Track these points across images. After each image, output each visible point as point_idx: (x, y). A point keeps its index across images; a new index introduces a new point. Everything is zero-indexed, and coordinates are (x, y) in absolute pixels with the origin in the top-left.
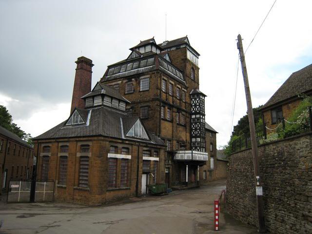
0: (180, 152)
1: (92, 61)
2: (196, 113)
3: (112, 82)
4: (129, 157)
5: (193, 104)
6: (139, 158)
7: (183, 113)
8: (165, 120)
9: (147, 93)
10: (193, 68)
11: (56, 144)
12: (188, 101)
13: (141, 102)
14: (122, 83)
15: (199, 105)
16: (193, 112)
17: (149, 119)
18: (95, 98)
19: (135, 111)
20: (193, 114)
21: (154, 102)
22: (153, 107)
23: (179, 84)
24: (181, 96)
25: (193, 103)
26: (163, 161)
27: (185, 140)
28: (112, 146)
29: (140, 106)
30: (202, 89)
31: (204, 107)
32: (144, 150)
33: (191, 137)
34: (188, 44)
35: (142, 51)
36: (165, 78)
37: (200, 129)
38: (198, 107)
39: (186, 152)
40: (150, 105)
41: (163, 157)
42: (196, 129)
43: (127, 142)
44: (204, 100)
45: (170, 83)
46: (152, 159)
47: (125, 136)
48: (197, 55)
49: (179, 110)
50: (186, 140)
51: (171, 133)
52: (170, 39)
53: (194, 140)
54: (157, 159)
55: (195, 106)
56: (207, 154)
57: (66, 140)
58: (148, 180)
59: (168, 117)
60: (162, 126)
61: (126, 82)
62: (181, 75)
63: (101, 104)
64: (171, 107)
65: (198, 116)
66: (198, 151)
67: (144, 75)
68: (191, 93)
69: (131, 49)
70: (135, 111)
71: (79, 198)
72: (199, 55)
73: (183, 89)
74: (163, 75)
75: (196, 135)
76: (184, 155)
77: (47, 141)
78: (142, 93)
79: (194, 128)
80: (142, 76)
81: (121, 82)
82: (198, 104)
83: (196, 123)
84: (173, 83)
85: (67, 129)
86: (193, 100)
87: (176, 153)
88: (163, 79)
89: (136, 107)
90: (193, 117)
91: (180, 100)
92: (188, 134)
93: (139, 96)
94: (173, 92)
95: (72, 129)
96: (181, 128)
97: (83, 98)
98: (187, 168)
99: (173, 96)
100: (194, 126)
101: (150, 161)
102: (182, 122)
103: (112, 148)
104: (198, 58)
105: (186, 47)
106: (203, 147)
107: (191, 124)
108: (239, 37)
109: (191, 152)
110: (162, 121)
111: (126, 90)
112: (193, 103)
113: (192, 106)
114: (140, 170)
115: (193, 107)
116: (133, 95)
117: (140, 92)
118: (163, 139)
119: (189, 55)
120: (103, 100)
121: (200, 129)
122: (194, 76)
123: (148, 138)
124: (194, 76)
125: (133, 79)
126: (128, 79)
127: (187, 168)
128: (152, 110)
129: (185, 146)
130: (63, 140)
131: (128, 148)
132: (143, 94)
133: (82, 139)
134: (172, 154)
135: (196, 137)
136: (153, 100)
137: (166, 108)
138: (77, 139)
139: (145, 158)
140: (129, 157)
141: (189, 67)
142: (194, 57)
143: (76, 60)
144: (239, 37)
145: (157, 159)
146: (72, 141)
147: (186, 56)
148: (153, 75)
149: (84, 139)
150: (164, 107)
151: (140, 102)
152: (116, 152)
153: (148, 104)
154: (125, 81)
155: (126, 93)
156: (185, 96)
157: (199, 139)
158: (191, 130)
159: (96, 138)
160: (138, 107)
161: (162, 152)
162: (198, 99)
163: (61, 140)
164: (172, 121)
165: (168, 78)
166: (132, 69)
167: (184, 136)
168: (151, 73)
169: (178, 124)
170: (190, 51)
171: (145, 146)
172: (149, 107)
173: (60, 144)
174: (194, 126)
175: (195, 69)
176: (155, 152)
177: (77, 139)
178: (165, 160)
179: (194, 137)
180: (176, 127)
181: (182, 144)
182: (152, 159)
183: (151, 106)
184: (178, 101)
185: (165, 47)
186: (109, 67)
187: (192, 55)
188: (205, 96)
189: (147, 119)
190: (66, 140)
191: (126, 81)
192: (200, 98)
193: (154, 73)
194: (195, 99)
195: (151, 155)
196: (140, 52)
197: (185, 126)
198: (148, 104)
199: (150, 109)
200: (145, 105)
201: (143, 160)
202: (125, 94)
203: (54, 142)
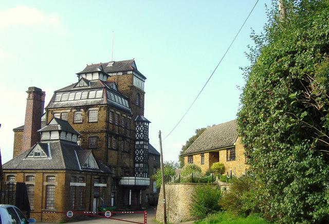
0: (125, 178)
2: (140, 140)
3: (61, 110)
4: (84, 185)
5: (137, 131)
6: (91, 185)
8: (111, 149)
9: (95, 124)
10: (138, 94)
11: (22, 174)
12: (132, 128)
15: (143, 132)
16: (137, 138)
18: (52, 133)
20: (137, 140)
23: (124, 114)
24: (126, 124)
25: (138, 129)
26: (110, 186)
27: (128, 165)
28: (72, 177)
29: (88, 136)
30: (147, 115)
31: (148, 133)
32: (95, 178)
33: (135, 162)
34: (135, 70)
35: (89, 77)
36: (112, 110)
37: (143, 155)
38: (142, 134)
39: (130, 178)
41: (110, 183)
42: (139, 155)
43: (83, 173)
44: (148, 126)
46: (101, 185)
47: (82, 168)
48: (143, 78)
49: (124, 138)
50: (130, 166)
51: (116, 160)
52: (117, 60)
53: (137, 165)
54: (105, 185)
55: (140, 132)
56: (149, 179)
57: (33, 171)
58: (98, 203)
59: (114, 146)
60: (109, 155)
63: (58, 138)
64: (116, 136)
65: (142, 143)
66: (141, 176)
67: (93, 107)
69: (79, 74)
71: (46, 218)
72: (145, 78)
73: (128, 117)
75: (139, 161)
76: (129, 181)
77: (12, 171)
78: (90, 124)
82: (142, 131)
83: (139, 150)
84: (119, 113)
85: (30, 160)
86: (138, 126)
87: (121, 179)
88: (111, 111)
89: (85, 136)
90: (137, 143)
91: (125, 128)
92: (132, 160)
94: (119, 122)
95: (36, 161)
96: (125, 155)
98: (130, 192)
99: (119, 126)
100: (137, 152)
101: (99, 187)
102: (127, 149)
103: (72, 178)
105: (132, 74)
106: (146, 172)
107: (135, 150)
108: (160, 131)
109: (134, 178)
110: (109, 150)
112: (138, 129)
114: (93, 195)
115: (138, 134)
116: (82, 125)
117: (88, 122)
118: (110, 167)
119: (136, 82)
120: (60, 135)
121: (143, 155)
122: (139, 102)
124: (139, 102)
126: (76, 109)
127: (130, 192)
128: (100, 141)
129: (129, 172)
130: (28, 171)
131: (83, 178)
133: (48, 171)
134: (117, 180)
135: (139, 162)
136: (101, 132)
138: (44, 171)
139: (96, 185)
140: (84, 185)
141: (135, 93)
142: (141, 82)
143: (27, 90)
144: (160, 131)
145: (105, 185)
146: (39, 172)
147: (132, 83)
149: (50, 171)
150: (111, 137)
151: (89, 133)
152: (75, 181)
153: (96, 135)
154: (74, 111)
156: (130, 123)
157: (142, 165)
158: (135, 156)
159: (62, 171)
161: (109, 178)
162: (142, 126)
163: (26, 171)
164: (117, 150)
165: (115, 110)
167: (128, 162)
169: (124, 152)
171: (96, 175)
172: (98, 137)
173: (26, 175)
175: (140, 94)
176: (104, 179)
177: (44, 171)
178: (111, 186)
180: (121, 154)
181: (127, 170)
182: (101, 185)
184: (124, 129)
186: (56, 92)
187: (138, 80)
188: (148, 122)
190: (33, 171)
191: (75, 110)
192: (144, 125)
194: (140, 126)
195: (100, 182)
197: (129, 153)
198: (96, 135)
200: (93, 135)
201: (95, 187)
203: (20, 172)
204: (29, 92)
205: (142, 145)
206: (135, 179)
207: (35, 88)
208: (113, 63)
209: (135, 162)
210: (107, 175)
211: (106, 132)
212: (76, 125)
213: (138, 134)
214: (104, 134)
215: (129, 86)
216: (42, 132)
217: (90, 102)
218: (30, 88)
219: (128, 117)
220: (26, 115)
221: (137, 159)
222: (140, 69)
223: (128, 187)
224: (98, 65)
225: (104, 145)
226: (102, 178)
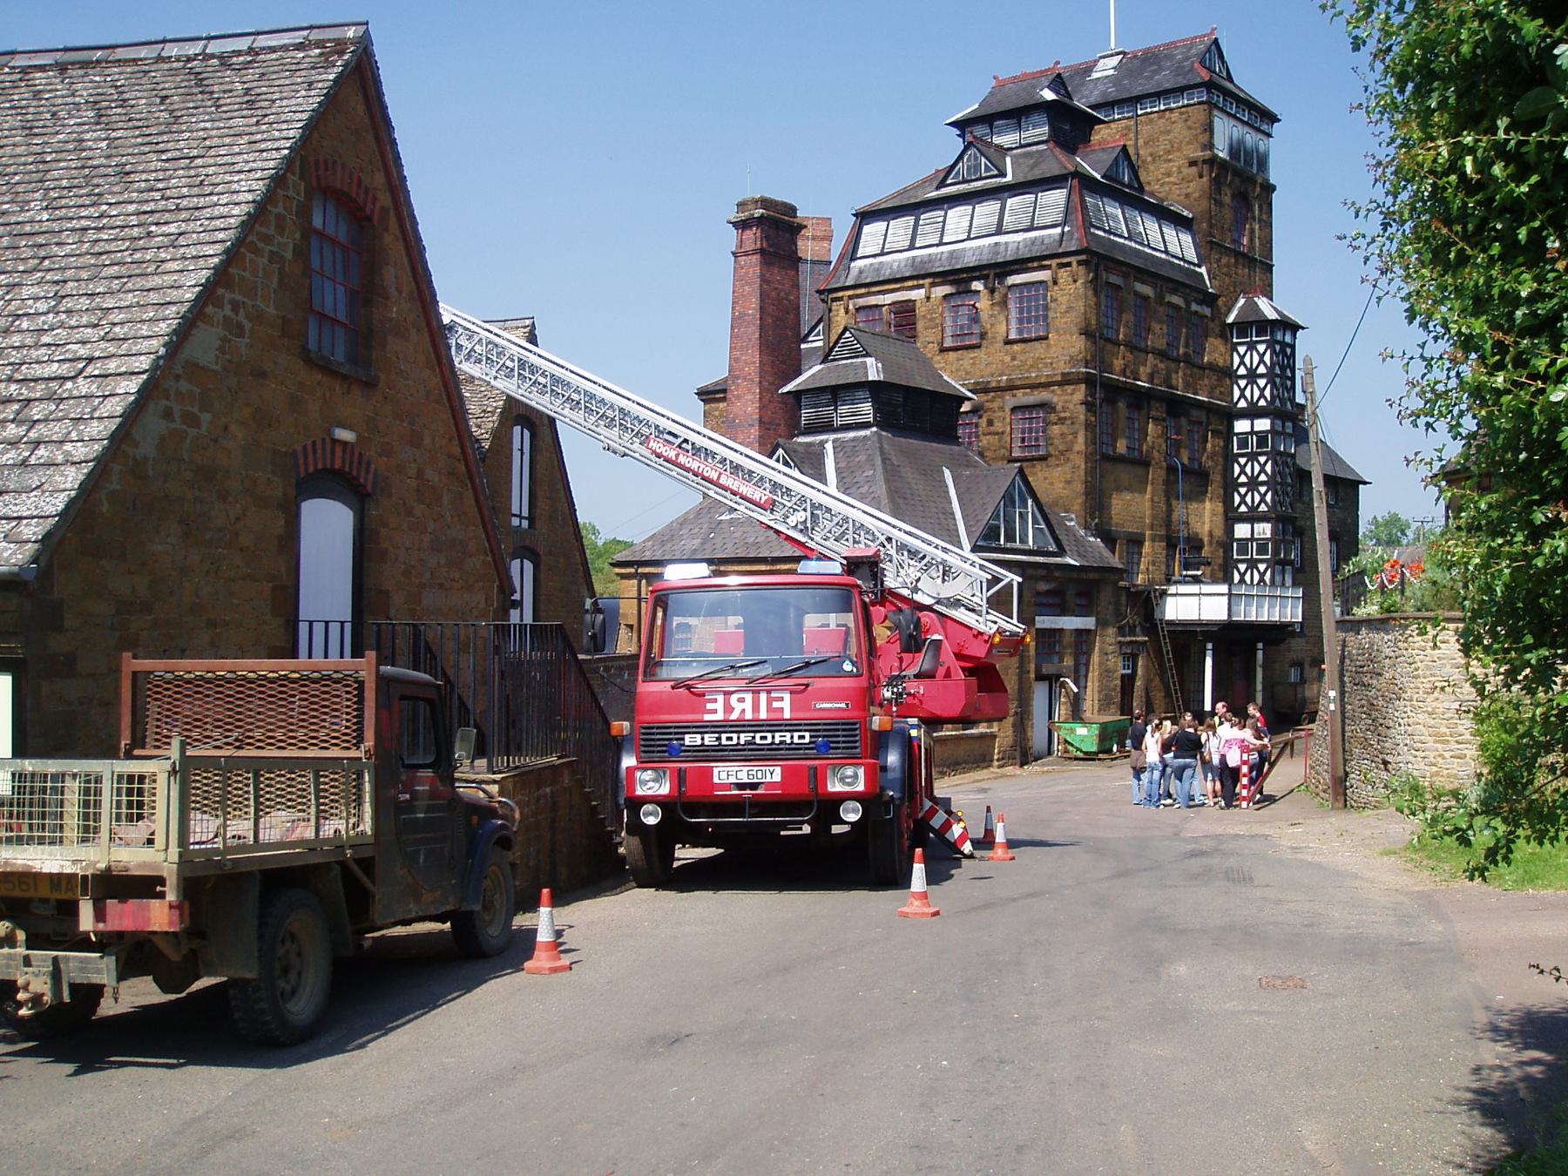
0: (1183, 589)
1: (791, 210)
5: (1242, 371)
7: (1195, 413)
13: (1018, 387)
14: (928, 298)
16: (1242, 404)
17: (1052, 461)
19: (990, 423)
20: (1243, 414)
21: (1069, 388)
22: (1064, 409)
29: (1010, 401)
36: (1114, 279)
39: (1206, 589)
40: (1055, 399)
42: (1253, 484)
44: (1293, 347)
45: (1137, 294)
48: (1263, 118)
53: (1242, 531)
61: (945, 297)
62: (1187, 239)
68: (1230, 320)
70: (990, 423)
72: (1273, 119)
73: (1194, 307)
74: (1107, 270)
75: (1253, 509)
78: (1015, 347)
79: (1243, 479)
80: (1018, 272)
81: (922, 291)
83: (1252, 457)
87: (1164, 594)
89: (995, 405)
90: (1242, 426)
93: (1008, 359)
97: (788, 393)
101: (1061, 630)
104: (1269, 135)
105: (1208, 103)
107: (1230, 459)
109: (1224, 588)
111: (948, 332)
112: (1242, 363)
113: (1231, 375)
117: (1008, 342)
123: (1053, 548)
125: (977, 285)
128: (1062, 421)
132: (1023, 352)
134: (1147, 603)
135: (1253, 517)
136: (1066, 381)
137: (1121, 405)
142: (1251, 138)
143: (734, 215)
148: (1063, 274)
151: (1011, 388)
155: (948, 343)
158: (1230, 485)
160: (1001, 409)
165: (1125, 276)
166: (969, 238)
168: (1054, 262)
170: (1229, 115)
171: (1043, 578)
174: (1243, 472)
176: (1079, 594)
179: (1243, 519)
183: (1059, 408)
185: (1113, 93)
186: (865, 216)
188: (1294, 328)
189: (1043, 459)
191: (947, 289)
193: (1069, 264)
195: (1064, 611)
196: (997, 140)
199: (1053, 417)
202: (943, 350)
204: (742, 225)
205: (1262, 438)
206: (1230, 595)
207: (765, 203)
208: (1115, 60)
209: (1231, 517)
210: (1092, 576)
211: (1089, 380)
212: (952, 355)
213: (1242, 383)
214: (1080, 392)
215: (1192, 163)
216: (797, 395)
217: (1014, 242)
218: (741, 205)
219: (1194, 307)
220: (736, 322)
221: (1244, 500)
222: (1248, 80)
223: (1191, 636)
224: (1043, 73)
225: (1081, 439)
226: (1070, 593)
